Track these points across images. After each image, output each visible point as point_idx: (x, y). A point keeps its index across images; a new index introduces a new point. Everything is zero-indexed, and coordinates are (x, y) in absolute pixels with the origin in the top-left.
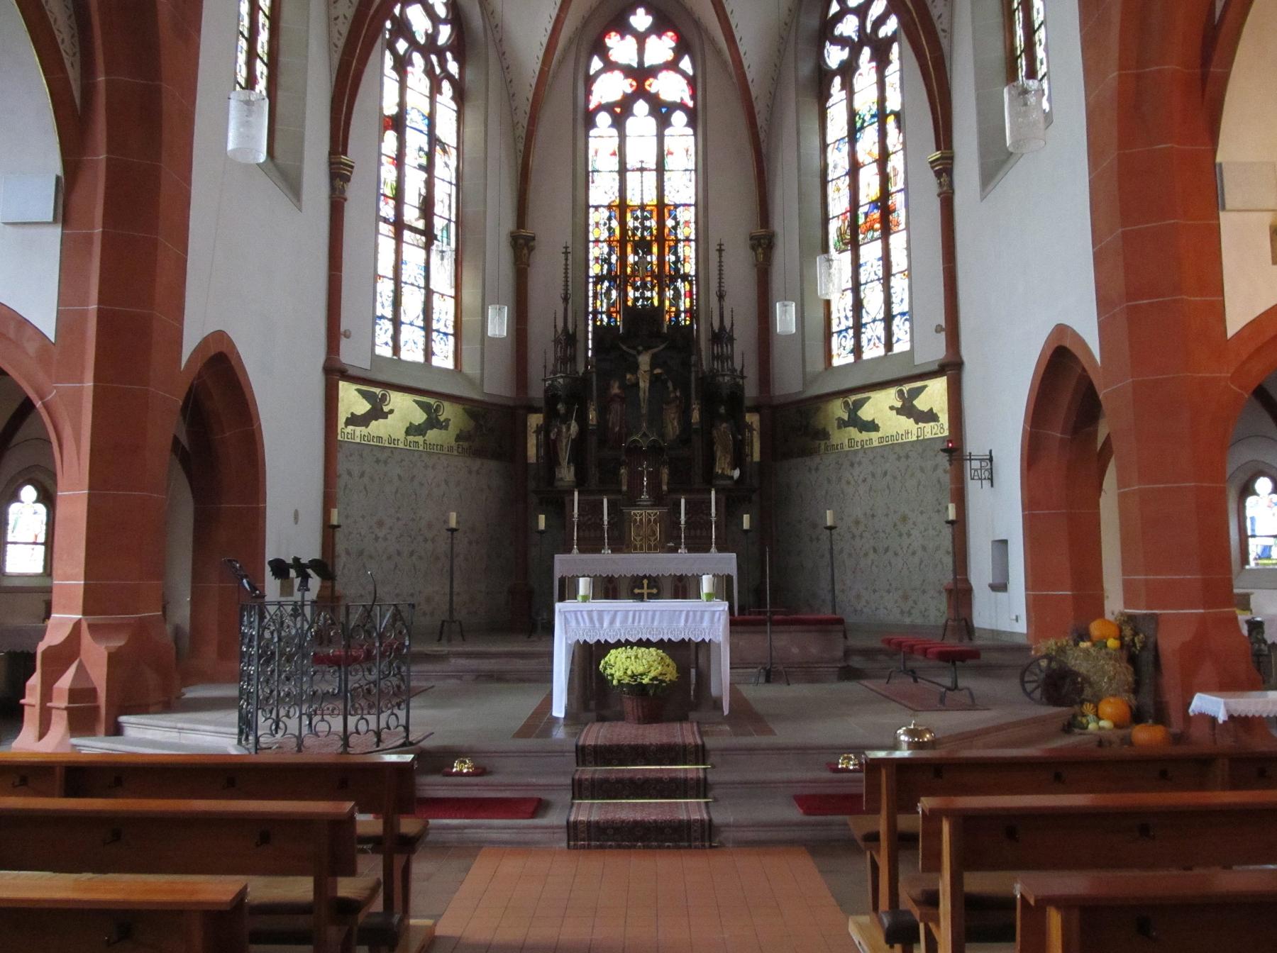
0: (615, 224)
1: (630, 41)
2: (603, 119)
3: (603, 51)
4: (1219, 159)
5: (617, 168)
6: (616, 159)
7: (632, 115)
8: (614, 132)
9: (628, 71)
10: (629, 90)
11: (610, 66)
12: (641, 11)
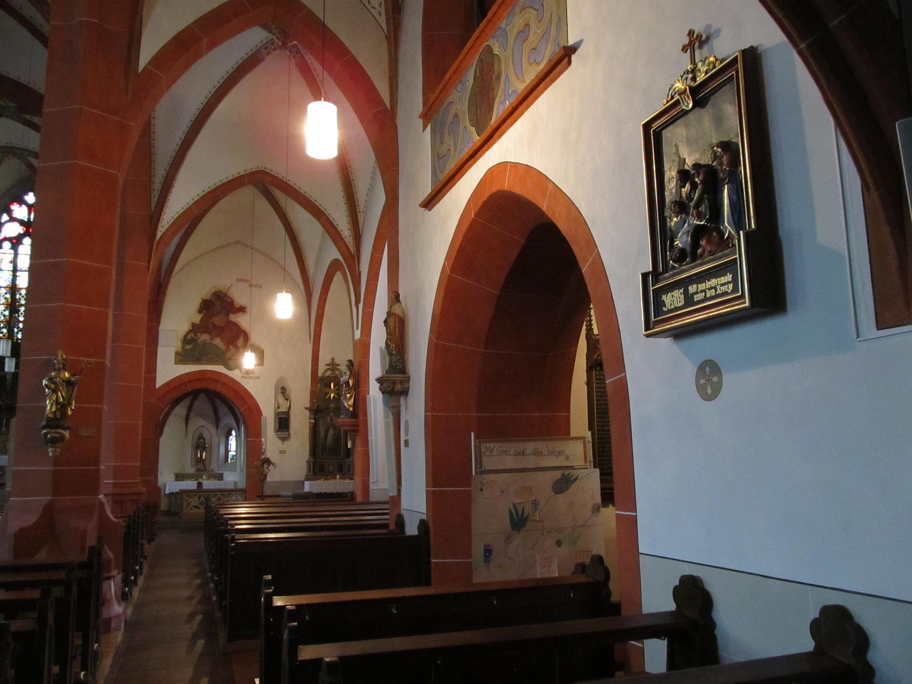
0: (8, 296)
1: (24, 209)
2: (7, 245)
3: (9, 212)
4: (160, 328)
5: (12, 269)
6: (11, 265)
7: (21, 243)
8: (12, 251)
9: (22, 222)
10: (22, 232)
11: (12, 219)
12: (31, 194)
